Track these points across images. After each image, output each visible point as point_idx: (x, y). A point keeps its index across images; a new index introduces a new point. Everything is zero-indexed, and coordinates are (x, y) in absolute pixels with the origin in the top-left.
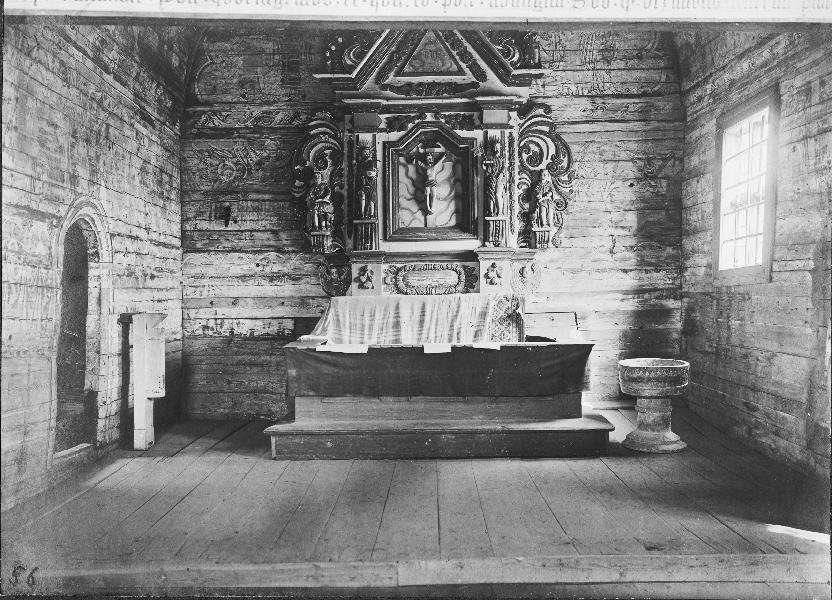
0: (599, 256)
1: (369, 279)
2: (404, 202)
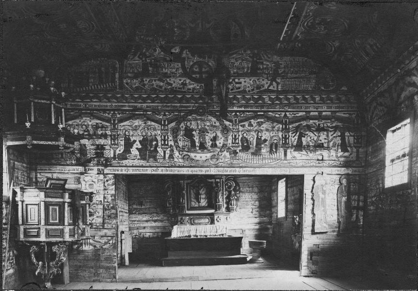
1: (183, 221)
2: (193, 200)
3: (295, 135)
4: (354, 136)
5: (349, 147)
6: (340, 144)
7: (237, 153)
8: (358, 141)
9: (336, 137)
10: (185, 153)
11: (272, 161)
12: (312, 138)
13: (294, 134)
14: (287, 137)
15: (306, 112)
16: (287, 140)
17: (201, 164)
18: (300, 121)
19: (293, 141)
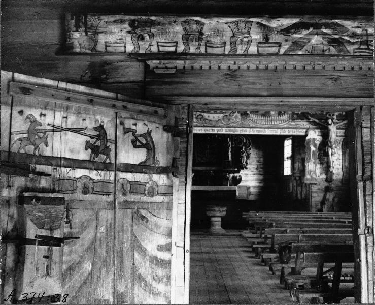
0: (253, 170)
7: (248, 114)
10: (199, 113)
11: (280, 122)
17: (213, 124)
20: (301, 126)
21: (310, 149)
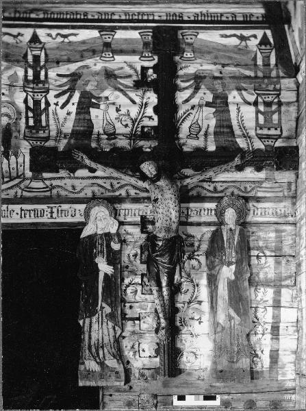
3: (67, 102)
4: (256, 104)
5: (239, 137)
6: (211, 130)
8: (268, 124)
9: (200, 106)
12: (123, 111)
13: (65, 97)
14: (43, 106)
15: (101, 29)
16: (43, 117)
18: (82, 58)
19: (61, 120)
20: (63, 193)
21: (96, 270)
